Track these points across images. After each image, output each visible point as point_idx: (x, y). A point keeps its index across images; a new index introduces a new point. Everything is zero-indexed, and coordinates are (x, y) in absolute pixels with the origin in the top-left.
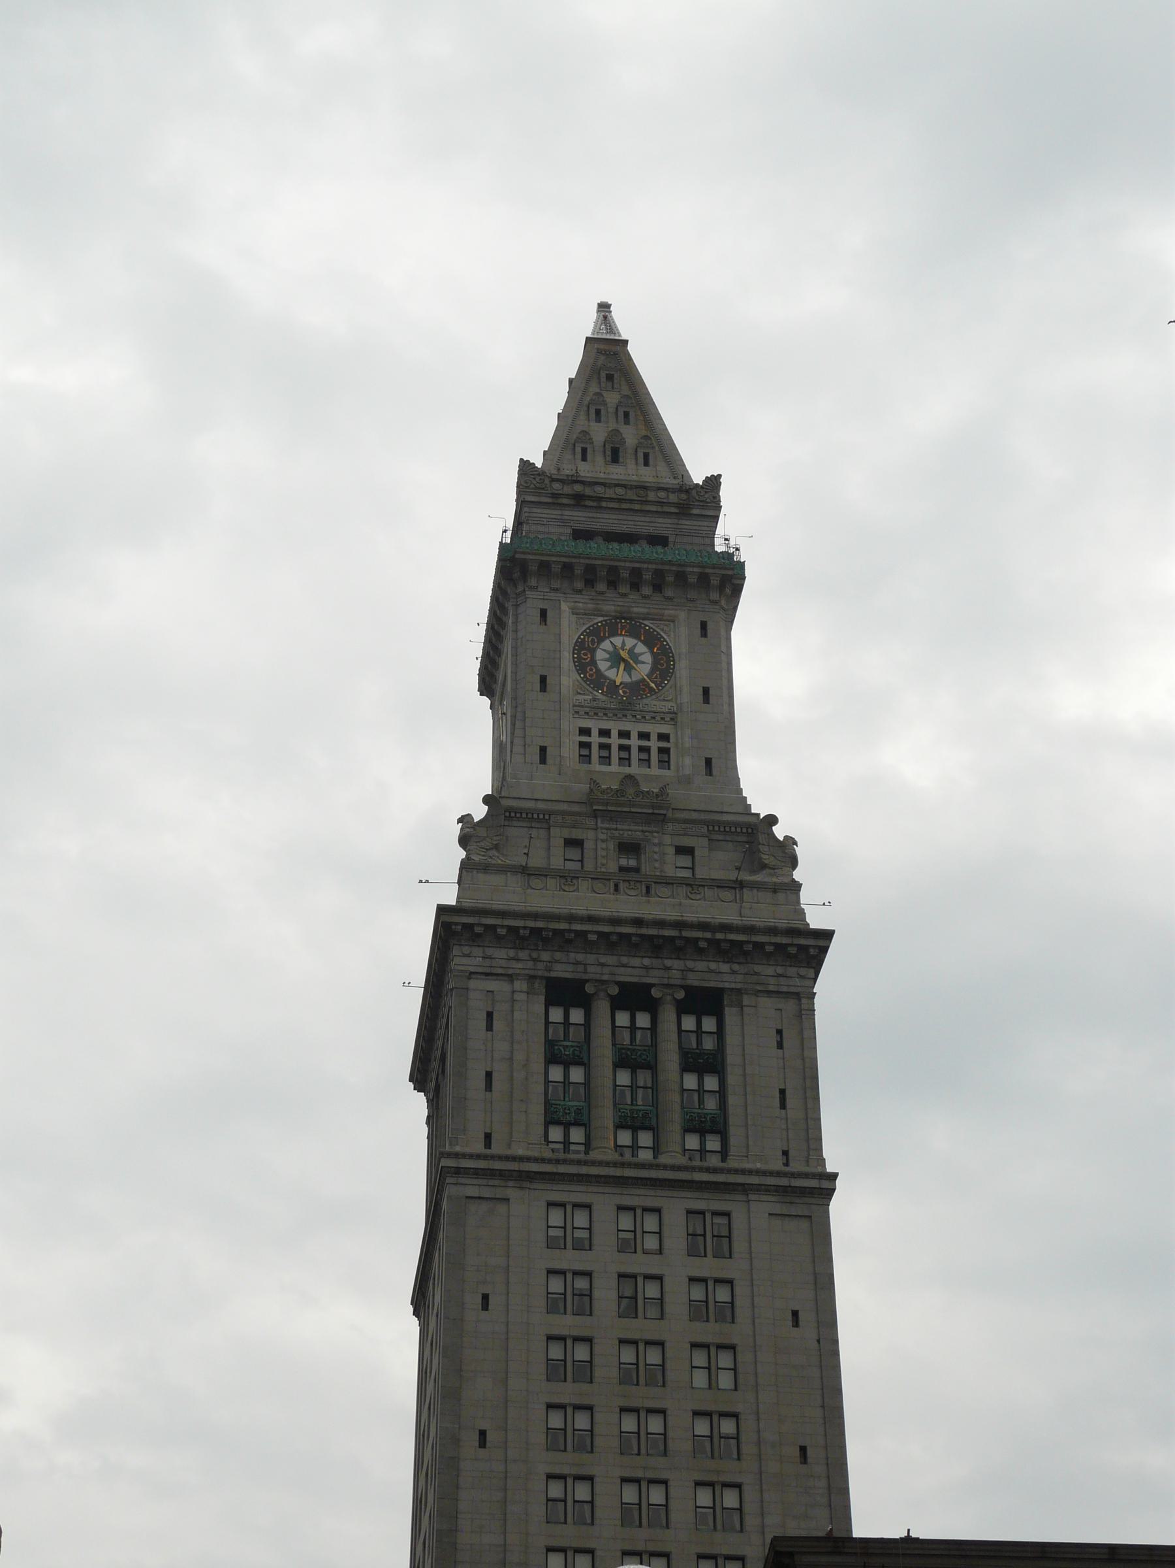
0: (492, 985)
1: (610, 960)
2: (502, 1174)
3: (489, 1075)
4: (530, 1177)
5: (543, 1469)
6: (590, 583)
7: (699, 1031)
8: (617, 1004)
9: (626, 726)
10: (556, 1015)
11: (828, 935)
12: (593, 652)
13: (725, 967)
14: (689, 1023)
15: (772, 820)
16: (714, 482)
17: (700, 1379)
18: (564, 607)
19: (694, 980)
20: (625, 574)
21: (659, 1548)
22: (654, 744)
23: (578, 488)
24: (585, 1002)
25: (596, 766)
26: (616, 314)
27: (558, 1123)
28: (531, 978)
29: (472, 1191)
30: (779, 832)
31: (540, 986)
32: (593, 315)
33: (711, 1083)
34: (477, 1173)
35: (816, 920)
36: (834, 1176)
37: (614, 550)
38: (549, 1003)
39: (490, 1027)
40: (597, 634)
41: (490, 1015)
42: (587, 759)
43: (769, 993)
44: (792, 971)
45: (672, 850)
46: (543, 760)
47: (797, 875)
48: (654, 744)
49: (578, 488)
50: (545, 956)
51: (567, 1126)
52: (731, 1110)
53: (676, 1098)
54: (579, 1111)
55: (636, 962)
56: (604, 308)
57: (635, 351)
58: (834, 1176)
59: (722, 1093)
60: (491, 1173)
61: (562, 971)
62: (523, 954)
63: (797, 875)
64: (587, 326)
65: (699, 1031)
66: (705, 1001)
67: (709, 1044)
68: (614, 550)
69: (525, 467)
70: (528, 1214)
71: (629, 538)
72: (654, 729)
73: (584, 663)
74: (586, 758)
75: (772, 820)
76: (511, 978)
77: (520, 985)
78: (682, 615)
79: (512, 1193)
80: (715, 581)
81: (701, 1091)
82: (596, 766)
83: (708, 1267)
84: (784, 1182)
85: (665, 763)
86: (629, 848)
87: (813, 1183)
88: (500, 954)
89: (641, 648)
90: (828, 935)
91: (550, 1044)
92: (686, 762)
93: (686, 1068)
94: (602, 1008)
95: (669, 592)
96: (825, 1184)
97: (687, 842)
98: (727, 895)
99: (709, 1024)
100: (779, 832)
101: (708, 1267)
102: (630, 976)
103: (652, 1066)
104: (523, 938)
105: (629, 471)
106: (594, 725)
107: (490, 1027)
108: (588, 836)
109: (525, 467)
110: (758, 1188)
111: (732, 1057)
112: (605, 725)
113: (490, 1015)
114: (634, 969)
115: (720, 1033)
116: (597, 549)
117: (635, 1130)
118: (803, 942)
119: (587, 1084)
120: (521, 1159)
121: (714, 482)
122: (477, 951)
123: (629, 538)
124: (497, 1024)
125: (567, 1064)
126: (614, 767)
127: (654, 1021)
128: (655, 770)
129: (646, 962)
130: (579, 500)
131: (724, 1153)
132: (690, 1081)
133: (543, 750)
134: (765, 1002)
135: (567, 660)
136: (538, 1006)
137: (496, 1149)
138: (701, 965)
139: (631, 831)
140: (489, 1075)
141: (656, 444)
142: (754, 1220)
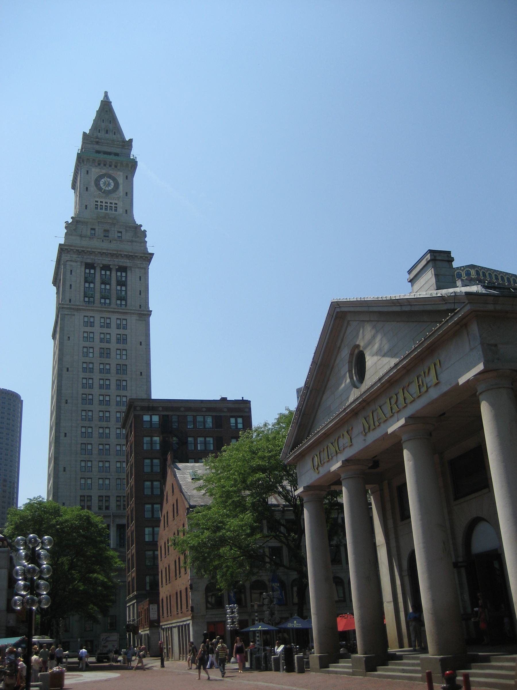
0: (72, 263)
1: (101, 258)
2: (73, 309)
3: (71, 285)
4: (80, 309)
5: (82, 376)
6: (99, 164)
7: (121, 276)
8: (102, 269)
9: (107, 201)
10: (87, 271)
11: (153, 254)
12: (99, 182)
13: (128, 261)
14: (119, 274)
15: (141, 226)
16: (131, 140)
17: (118, 357)
19: (121, 264)
20: (108, 163)
21: (108, 394)
22: (113, 205)
23: (97, 140)
24: (94, 268)
25: (99, 210)
26: (109, 95)
27: (87, 297)
28: (82, 262)
29: (66, 313)
30: (142, 229)
31: (83, 264)
32: (103, 95)
33: (124, 288)
34: (67, 308)
35: (150, 251)
36: (151, 311)
37: (106, 154)
38: (86, 268)
39: (71, 274)
40: (101, 177)
41: (71, 271)
42: (97, 208)
43: (138, 268)
44: (144, 262)
45: (116, 232)
46: (86, 208)
47: (146, 239)
48: (113, 205)
49: (97, 140)
50: (85, 257)
51: (89, 298)
52: (128, 295)
53: (115, 292)
54: (92, 294)
55: (107, 259)
56: (106, 93)
57: (113, 105)
58: (151, 311)
59: (126, 291)
60: (71, 308)
61: (89, 261)
62: (80, 256)
63: (146, 239)
64: (102, 97)
65: (121, 276)
66: (123, 269)
67: (124, 279)
68: (106, 154)
69: (84, 134)
70: (78, 319)
71: (109, 153)
72: (114, 202)
73: (97, 184)
74: (97, 208)
75: (141, 226)
76: (76, 262)
77: (79, 263)
78: (121, 173)
79: (75, 313)
80: (130, 166)
81: (121, 290)
82: (99, 210)
83: (121, 331)
84: (139, 312)
85: (116, 210)
86: (106, 231)
87: (146, 313)
88: (75, 256)
89: (111, 181)
90: (153, 254)
92: (120, 211)
93: (118, 285)
94: (98, 270)
95: (118, 167)
96: (149, 313)
97: (120, 230)
98: (129, 243)
99: (124, 274)
100: (142, 229)
101: (121, 331)
103: (110, 284)
104: (80, 252)
105: (110, 136)
106: (99, 200)
107: (71, 274)
108: (97, 228)
109: (84, 134)
110: (133, 313)
111: (129, 283)
112: (102, 200)
113: (71, 271)
114: (106, 261)
115: (126, 277)
116: (101, 156)
117: (105, 299)
118: (147, 256)
119: (94, 288)
120: (78, 306)
121: (131, 140)
122: (68, 255)
123: (109, 153)
124: (73, 273)
125: (90, 283)
126: (103, 211)
127: (111, 273)
128: (113, 212)
129: (109, 259)
130: (97, 143)
131: (126, 305)
132: (119, 288)
133: (86, 206)
134: (137, 270)
135: (93, 183)
136: (83, 269)
137: (72, 303)
138: (122, 260)
139: (107, 227)
140: (71, 285)
141: (117, 130)
142: (132, 320)
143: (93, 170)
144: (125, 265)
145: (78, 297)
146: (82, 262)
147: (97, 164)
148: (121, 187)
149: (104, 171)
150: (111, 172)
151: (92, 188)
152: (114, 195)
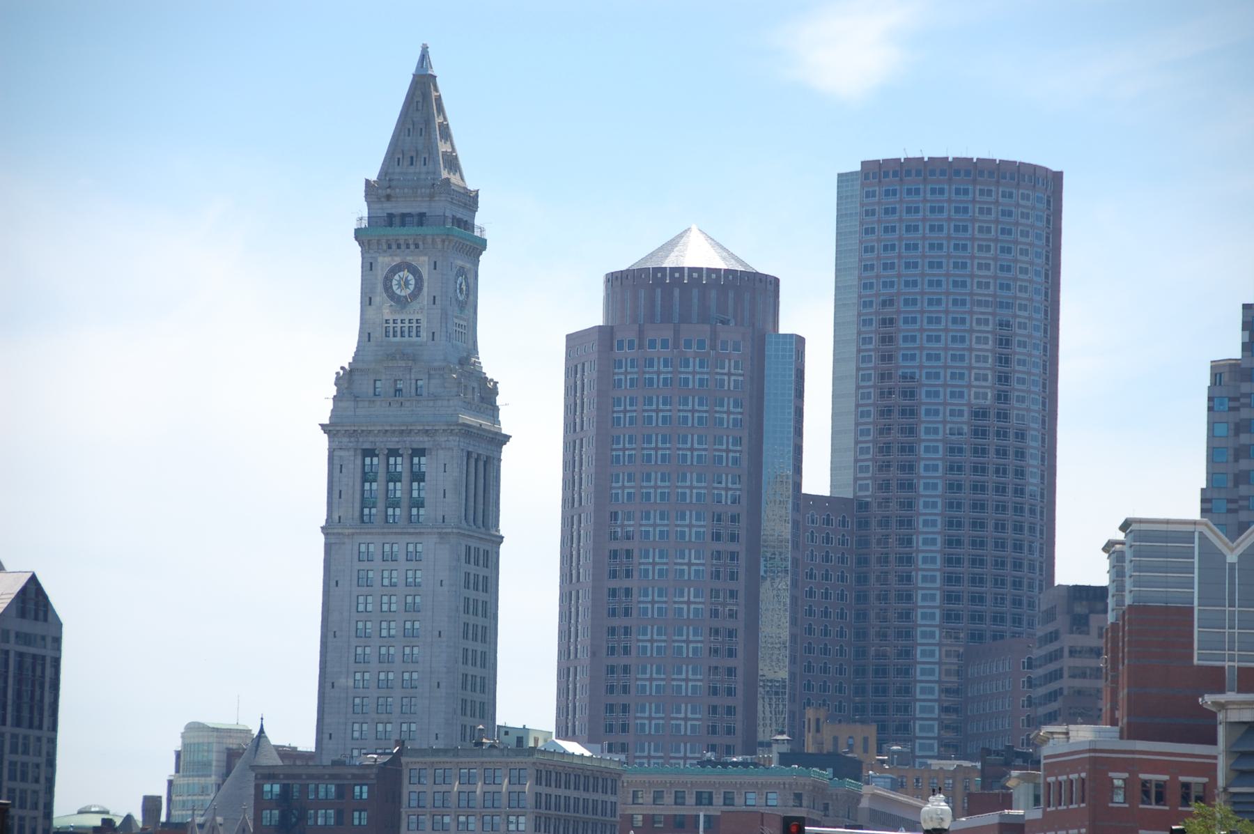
0: (342, 453)
13: (426, 439)
18: (380, 259)
19: (415, 446)
31: (359, 452)
48: (414, 325)
69: (367, 182)
76: (348, 450)
77: (352, 453)
78: (426, 259)
88: (345, 440)
91: (364, 473)
102: (391, 446)
109: (367, 182)
128: (414, 339)
134: (441, 452)
143: (380, 259)
144: (421, 446)
145: (351, 510)
146: (355, 450)
147: (385, 247)
148: (426, 284)
149: (398, 260)
150: (409, 259)
151: (380, 297)
152: (415, 305)
